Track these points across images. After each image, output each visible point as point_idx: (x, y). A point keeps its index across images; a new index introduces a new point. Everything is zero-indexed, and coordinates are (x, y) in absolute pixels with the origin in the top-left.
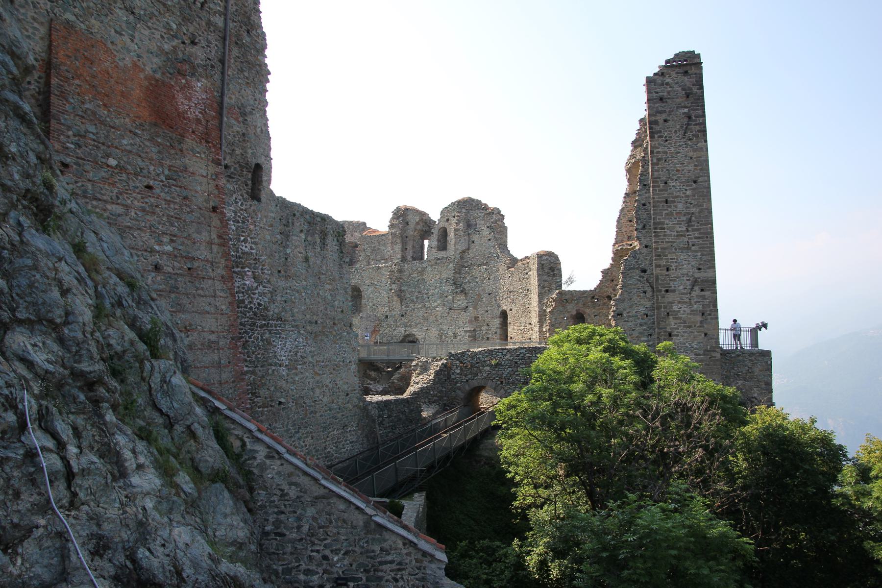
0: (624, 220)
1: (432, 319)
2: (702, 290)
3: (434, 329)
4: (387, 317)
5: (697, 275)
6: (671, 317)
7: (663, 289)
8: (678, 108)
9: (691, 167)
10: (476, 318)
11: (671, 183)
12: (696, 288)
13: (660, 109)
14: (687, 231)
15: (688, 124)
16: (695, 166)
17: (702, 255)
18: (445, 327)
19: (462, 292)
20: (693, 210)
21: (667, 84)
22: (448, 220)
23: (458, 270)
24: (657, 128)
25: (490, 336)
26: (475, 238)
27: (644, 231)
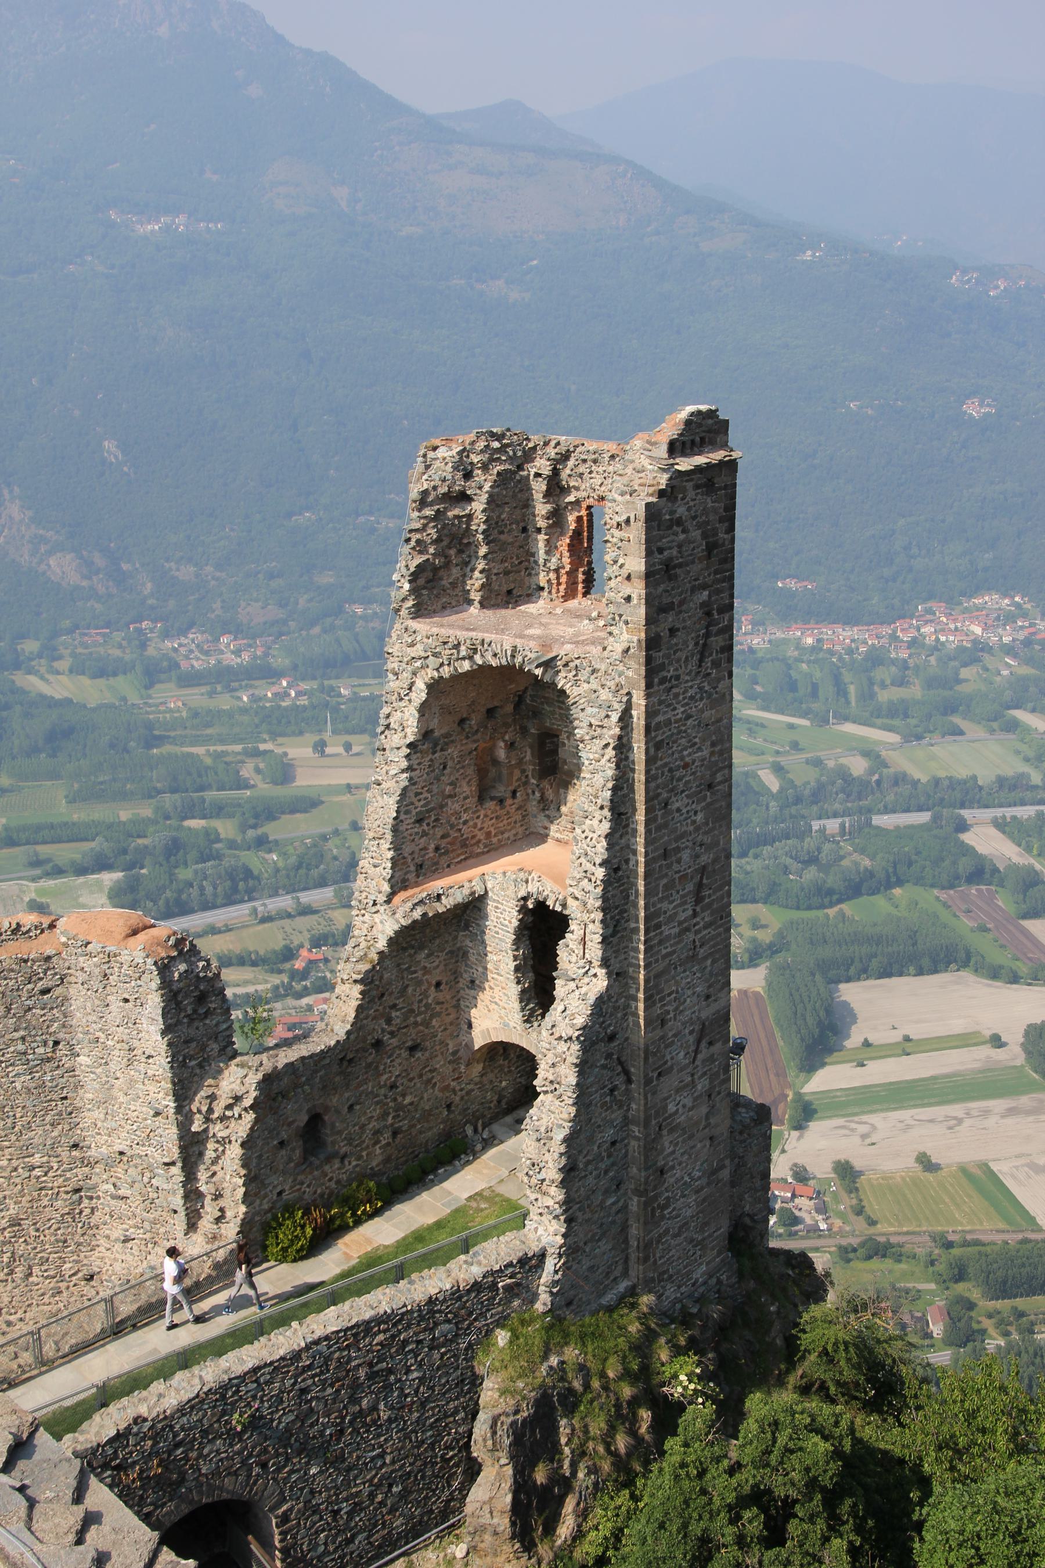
0: (409, 820)
2: (710, 1043)
5: (704, 1015)
6: (665, 1132)
7: (655, 1075)
8: (693, 590)
9: (705, 753)
12: (703, 1044)
13: (666, 600)
14: (695, 914)
15: (707, 635)
16: (713, 745)
17: (713, 962)
20: (705, 859)
21: (679, 522)
24: (659, 656)
27: (615, 940)
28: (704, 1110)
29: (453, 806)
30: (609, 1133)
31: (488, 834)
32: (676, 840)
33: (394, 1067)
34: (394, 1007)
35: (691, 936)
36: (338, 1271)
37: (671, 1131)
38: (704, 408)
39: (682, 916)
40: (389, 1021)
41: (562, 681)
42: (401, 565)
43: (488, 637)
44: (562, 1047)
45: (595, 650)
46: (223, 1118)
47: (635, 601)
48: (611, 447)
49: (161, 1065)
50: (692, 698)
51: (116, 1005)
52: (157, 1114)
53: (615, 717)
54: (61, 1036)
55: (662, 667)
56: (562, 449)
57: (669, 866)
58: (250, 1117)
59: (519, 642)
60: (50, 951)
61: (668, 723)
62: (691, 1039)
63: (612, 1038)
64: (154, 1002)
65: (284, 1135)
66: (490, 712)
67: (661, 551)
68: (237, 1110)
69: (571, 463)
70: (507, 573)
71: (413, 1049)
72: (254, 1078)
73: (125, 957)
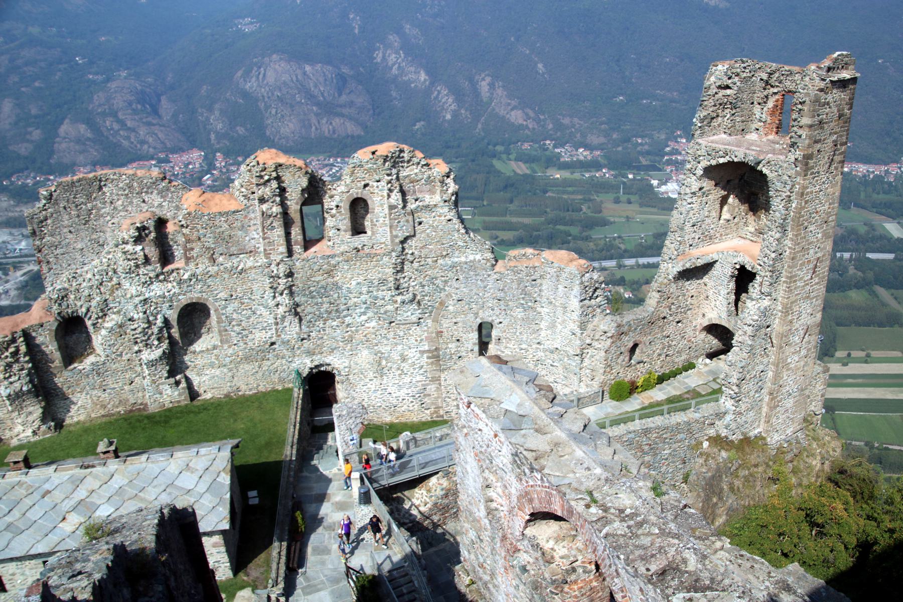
1: (359, 337)
3: (365, 352)
4: (273, 344)
8: (830, 134)
9: (826, 207)
10: (440, 333)
11: (812, 228)
14: (812, 278)
15: (834, 155)
16: (830, 204)
18: (384, 349)
19: (412, 301)
20: (819, 255)
21: (828, 104)
22: (366, 186)
23: (400, 269)
24: (811, 163)
25: (464, 354)
26: (424, 217)
28: (802, 363)
29: (708, 221)
30: (761, 367)
31: (721, 235)
32: (809, 244)
33: (670, 329)
34: (673, 304)
35: (808, 287)
36: (639, 407)
37: (788, 370)
38: (845, 53)
39: (806, 278)
40: (670, 310)
41: (765, 171)
42: (697, 116)
43: (734, 148)
44: (746, 328)
45: (782, 157)
46: (598, 340)
47: (804, 137)
48: (795, 69)
49: (575, 316)
50: (824, 183)
51: (561, 287)
52: (574, 334)
53: (788, 187)
54: (538, 299)
55: (813, 168)
56: (773, 68)
57: (803, 256)
58: (610, 340)
59: (747, 151)
60: (537, 264)
61: (812, 192)
62: (802, 332)
63: (768, 327)
64: (577, 289)
65: (623, 349)
66: (728, 181)
67: (818, 115)
68: (603, 338)
69: (777, 75)
70: (743, 122)
71: (678, 322)
72: (614, 325)
73: (567, 270)
